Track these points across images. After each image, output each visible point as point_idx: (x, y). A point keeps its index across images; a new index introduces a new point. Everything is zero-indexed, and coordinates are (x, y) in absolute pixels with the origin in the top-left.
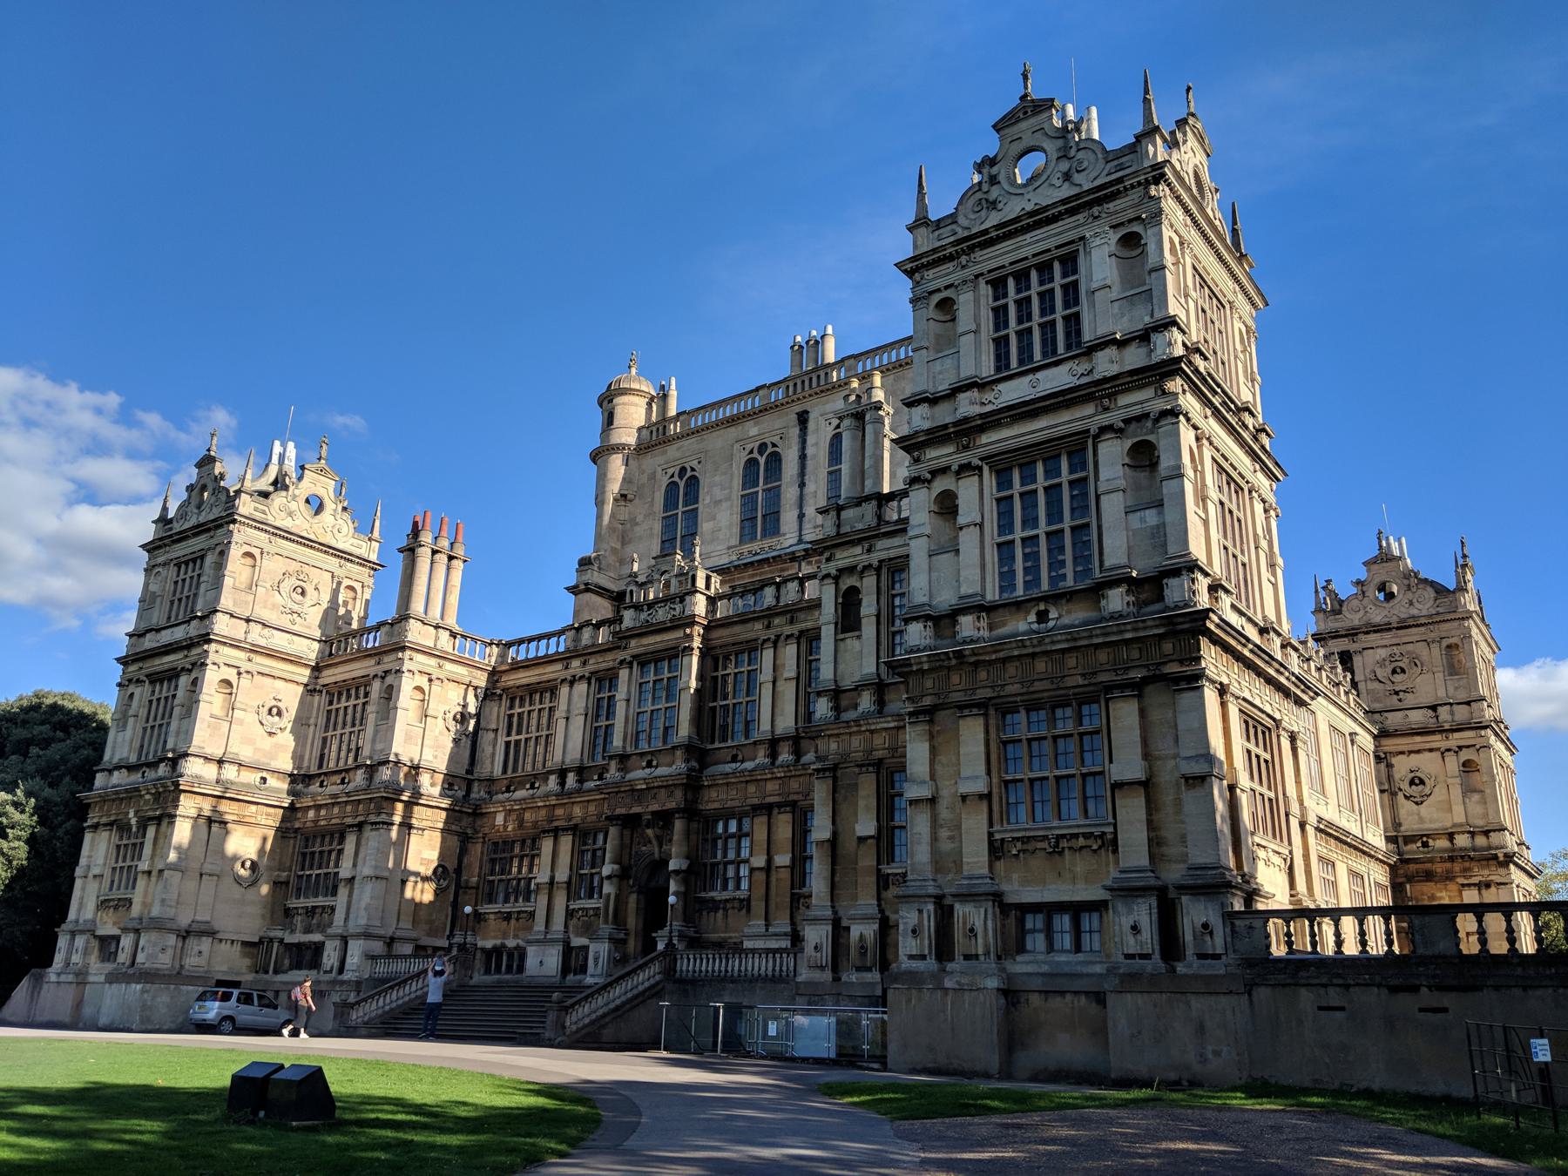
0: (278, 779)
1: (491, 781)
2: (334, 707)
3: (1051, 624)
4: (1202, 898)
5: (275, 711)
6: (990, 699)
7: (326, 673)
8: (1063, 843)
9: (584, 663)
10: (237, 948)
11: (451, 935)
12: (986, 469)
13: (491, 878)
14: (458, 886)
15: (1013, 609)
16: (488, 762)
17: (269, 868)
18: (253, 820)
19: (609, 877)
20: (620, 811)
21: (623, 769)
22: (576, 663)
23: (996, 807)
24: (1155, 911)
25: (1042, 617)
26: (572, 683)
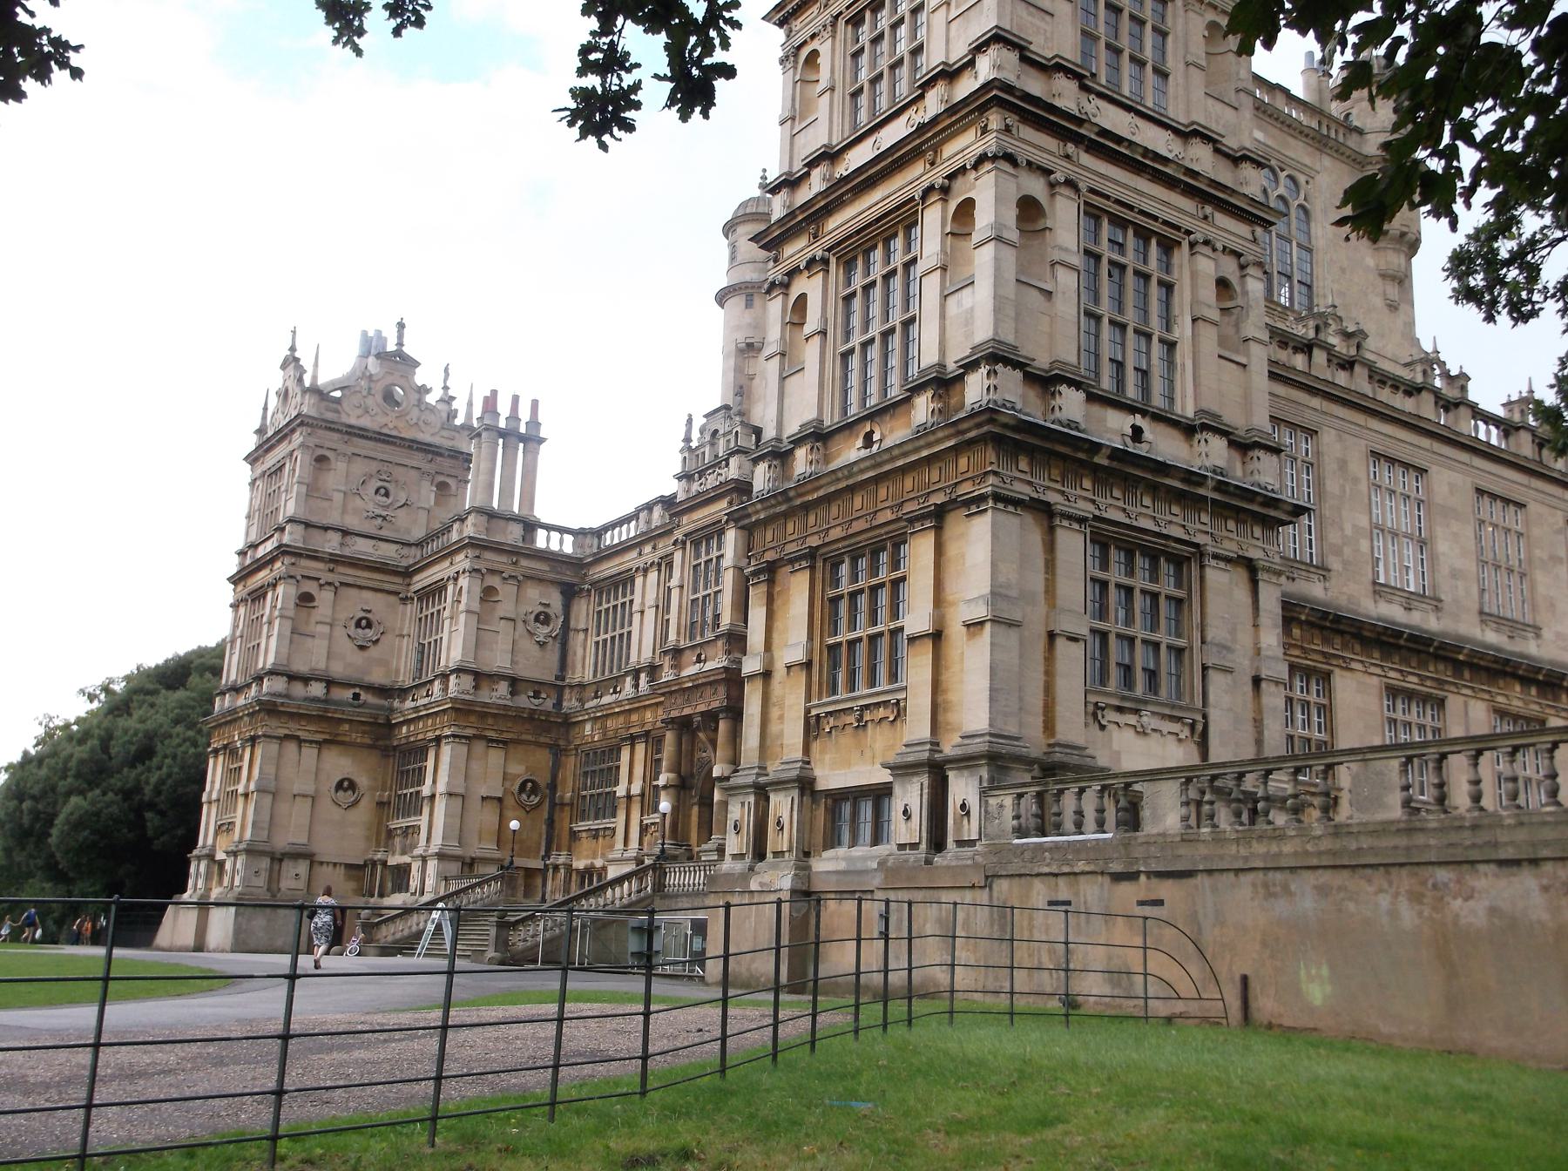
0: (373, 694)
1: (582, 686)
2: (424, 613)
3: (875, 447)
4: (966, 773)
5: (364, 623)
6: (818, 548)
7: (416, 578)
8: (867, 716)
9: (654, 548)
10: (341, 871)
11: (547, 856)
12: (833, 260)
13: (584, 793)
14: (553, 805)
15: (847, 432)
16: (579, 666)
17: (373, 789)
18: (347, 739)
19: (665, 787)
20: (674, 714)
21: (677, 666)
22: (648, 549)
23: (815, 678)
24: (926, 791)
25: (868, 441)
26: (646, 571)
